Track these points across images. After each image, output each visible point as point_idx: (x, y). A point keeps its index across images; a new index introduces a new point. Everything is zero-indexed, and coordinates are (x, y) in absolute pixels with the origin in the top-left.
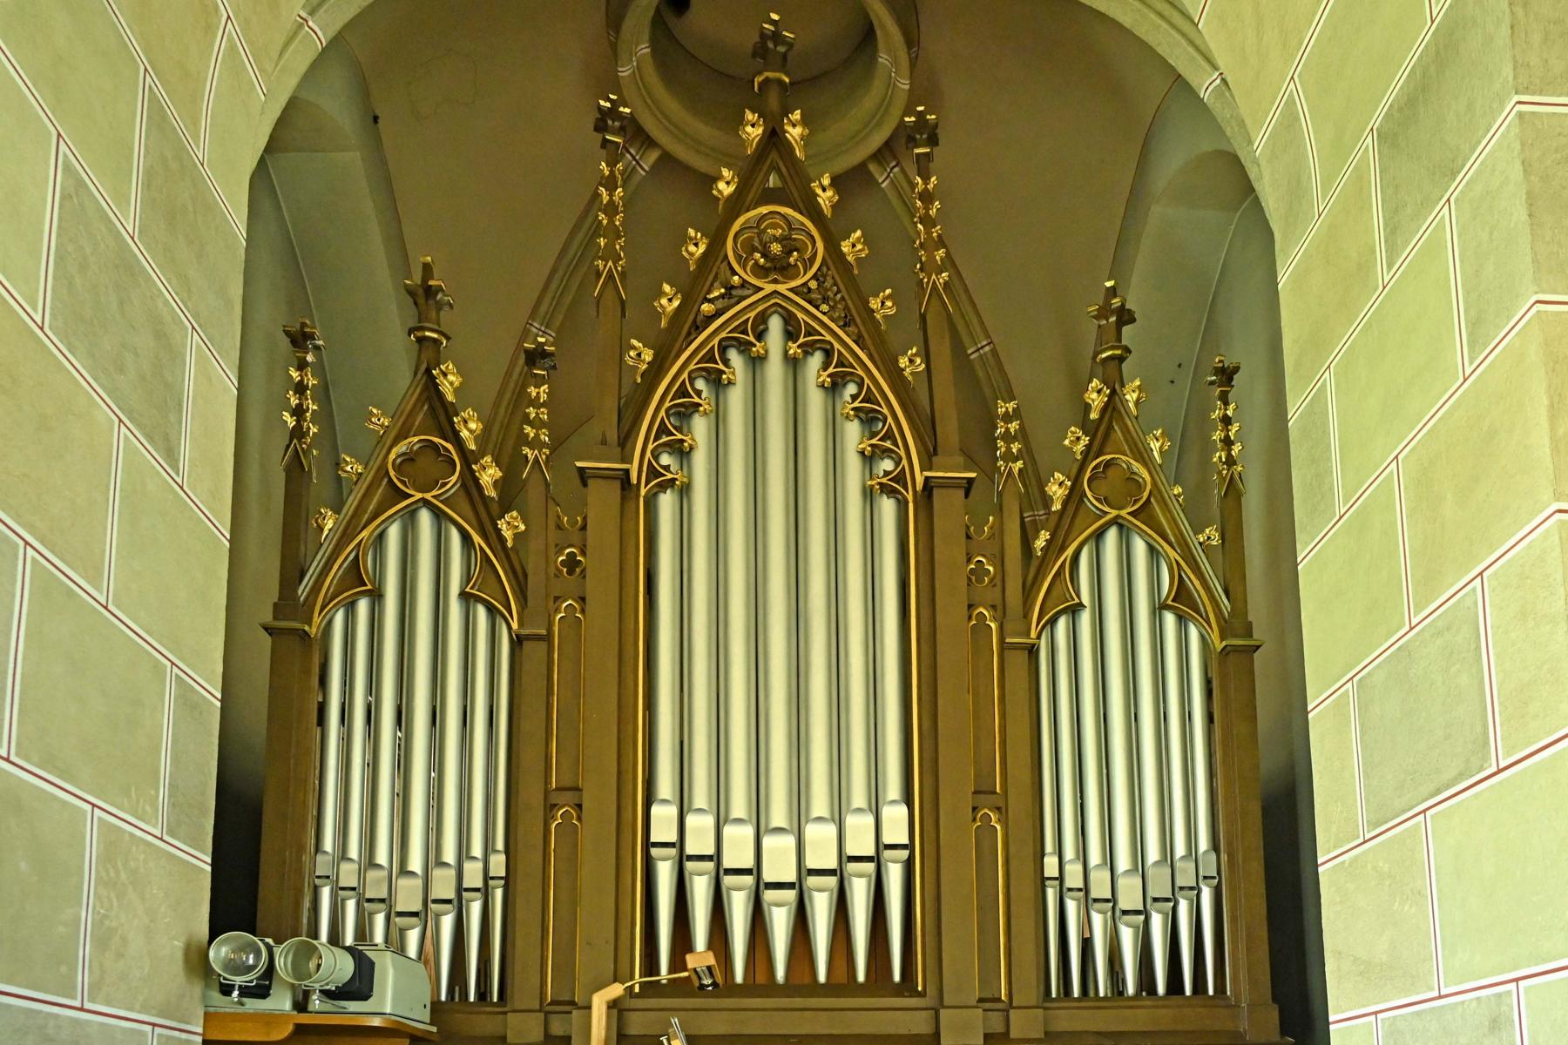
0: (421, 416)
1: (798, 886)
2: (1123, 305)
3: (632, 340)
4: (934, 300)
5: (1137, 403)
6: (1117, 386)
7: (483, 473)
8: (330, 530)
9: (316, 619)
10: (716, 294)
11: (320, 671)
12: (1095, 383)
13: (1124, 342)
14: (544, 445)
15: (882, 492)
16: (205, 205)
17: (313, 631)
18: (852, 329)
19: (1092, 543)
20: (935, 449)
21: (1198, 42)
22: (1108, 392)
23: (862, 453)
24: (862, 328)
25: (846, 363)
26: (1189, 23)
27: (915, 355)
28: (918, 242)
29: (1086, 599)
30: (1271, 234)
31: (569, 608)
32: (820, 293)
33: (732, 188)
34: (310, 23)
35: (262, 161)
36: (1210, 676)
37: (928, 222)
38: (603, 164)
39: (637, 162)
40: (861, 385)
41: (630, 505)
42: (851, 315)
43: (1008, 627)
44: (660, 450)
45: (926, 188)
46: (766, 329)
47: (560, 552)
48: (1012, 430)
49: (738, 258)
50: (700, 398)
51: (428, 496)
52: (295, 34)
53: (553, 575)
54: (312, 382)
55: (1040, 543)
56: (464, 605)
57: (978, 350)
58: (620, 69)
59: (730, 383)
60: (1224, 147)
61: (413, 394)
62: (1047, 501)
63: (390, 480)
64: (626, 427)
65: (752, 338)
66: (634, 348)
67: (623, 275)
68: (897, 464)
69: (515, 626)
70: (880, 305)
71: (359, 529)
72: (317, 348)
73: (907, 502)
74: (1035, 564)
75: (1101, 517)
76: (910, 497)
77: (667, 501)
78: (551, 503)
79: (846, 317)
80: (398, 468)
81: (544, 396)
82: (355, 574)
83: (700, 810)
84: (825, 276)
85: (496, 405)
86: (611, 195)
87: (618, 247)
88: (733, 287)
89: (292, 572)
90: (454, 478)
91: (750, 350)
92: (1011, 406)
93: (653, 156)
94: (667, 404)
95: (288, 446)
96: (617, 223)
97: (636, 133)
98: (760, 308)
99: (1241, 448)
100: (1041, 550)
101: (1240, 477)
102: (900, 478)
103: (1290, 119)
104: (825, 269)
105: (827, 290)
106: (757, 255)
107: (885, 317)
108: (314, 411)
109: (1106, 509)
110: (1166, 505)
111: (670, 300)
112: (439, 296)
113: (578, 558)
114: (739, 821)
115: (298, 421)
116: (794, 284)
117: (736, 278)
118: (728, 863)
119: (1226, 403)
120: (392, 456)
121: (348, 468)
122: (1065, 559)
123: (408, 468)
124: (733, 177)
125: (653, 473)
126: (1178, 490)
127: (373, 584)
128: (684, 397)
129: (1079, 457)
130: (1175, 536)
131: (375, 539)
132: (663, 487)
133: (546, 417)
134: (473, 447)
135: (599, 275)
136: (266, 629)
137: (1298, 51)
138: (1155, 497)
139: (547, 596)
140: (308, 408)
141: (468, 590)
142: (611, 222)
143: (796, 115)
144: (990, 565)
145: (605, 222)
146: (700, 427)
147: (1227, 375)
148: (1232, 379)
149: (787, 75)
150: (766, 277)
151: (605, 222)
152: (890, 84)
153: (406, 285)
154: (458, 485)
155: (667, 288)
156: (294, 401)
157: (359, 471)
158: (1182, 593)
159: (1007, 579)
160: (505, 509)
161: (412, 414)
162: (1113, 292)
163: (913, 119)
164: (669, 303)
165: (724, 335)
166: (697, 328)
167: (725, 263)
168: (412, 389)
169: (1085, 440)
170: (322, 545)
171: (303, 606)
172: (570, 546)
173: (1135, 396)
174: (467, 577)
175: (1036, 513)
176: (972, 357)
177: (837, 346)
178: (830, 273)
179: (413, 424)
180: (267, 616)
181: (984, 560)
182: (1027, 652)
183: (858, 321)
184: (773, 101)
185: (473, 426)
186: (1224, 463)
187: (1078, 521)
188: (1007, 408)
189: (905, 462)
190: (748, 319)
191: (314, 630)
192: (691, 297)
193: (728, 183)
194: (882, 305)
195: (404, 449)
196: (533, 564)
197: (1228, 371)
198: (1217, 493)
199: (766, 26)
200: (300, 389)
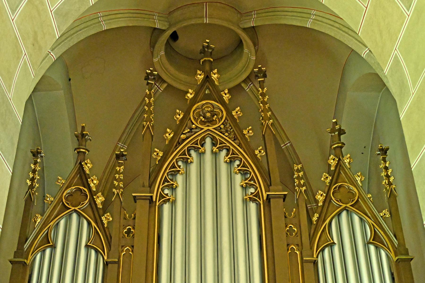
0: (76, 179)
2: (340, 128)
3: (155, 149)
4: (268, 129)
5: (349, 163)
6: (341, 157)
7: (97, 199)
8: (39, 222)
9: (30, 257)
10: (186, 131)
11: (29, 278)
12: (332, 156)
13: (342, 141)
14: (121, 188)
15: (250, 200)
16: (10, 111)
17: (28, 262)
18: (237, 141)
19: (336, 218)
20: (270, 184)
21: (359, 39)
22: (337, 159)
23: (242, 186)
24: (240, 140)
25: (235, 153)
26: (355, 34)
27: (261, 149)
28: (261, 110)
29: (336, 241)
30: (395, 101)
31: (128, 250)
32: (225, 129)
33: (192, 96)
34: (52, 53)
35: (31, 96)
36: (392, 271)
37: (264, 103)
38: (147, 90)
39: (159, 88)
40: (241, 161)
41: (153, 209)
42: (237, 136)
43: (304, 254)
44: (165, 188)
45: (263, 92)
46: (205, 143)
47: (125, 228)
48: (300, 175)
49: (195, 119)
50: (180, 168)
52: (46, 57)
53: (122, 237)
54: (38, 168)
55: (315, 219)
56: (87, 249)
57: (285, 145)
58: (154, 59)
59: (191, 162)
60: (372, 71)
61: (74, 172)
62: (317, 202)
63: (63, 203)
64: (152, 180)
65: (199, 146)
66: (156, 152)
67: (153, 127)
68: (256, 189)
69: (106, 258)
70: (247, 132)
71: (50, 222)
72: (42, 157)
73: (260, 204)
74: (313, 227)
75: (339, 207)
76: (261, 202)
77: (166, 207)
78: (122, 209)
79: (235, 137)
80: (66, 199)
81: (122, 170)
82: (46, 240)
84: (226, 123)
85: (104, 172)
86: (149, 100)
87: (151, 117)
88: (193, 129)
89: (23, 239)
90: (87, 201)
91: (199, 150)
92: (300, 166)
93: (165, 85)
94: (168, 171)
95: (27, 192)
96: (151, 109)
97: (159, 79)
98: (203, 135)
99: (393, 178)
100: (316, 221)
101: (395, 190)
102: (257, 195)
103: (397, 61)
104: (226, 121)
105: (227, 128)
106: (202, 117)
107: (249, 136)
108: (38, 179)
109: (341, 204)
110: (365, 201)
111: (170, 134)
112: (86, 137)
113: (132, 230)
115: (32, 183)
116: (215, 127)
117: (194, 126)
119: (385, 162)
120: (65, 194)
121: (48, 199)
122: (326, 224)
123: (70, 198)
124: (193, 92)
125: (162, 196)
126: (369, 196)
127: (53, 243)
128: (174, 168)
129: (328, 184)
130: (370, 213)
131: (55, 226)
132: (165, 202)
133: (122, 177)
134: (94, 189)
135: (144, 127)
136: (10, 262)
137: (397, 41)
138: (361, 199)
139: (119, 245)
140: (36, 178)
141: (88, 244)
142: (149, 109)
143: (216, 71)
144: (294, 228)
145: (147, 109)
146: (180, 179)
147: (384, 151)
148: (386, 153)
149: (212, 58)
150: (205, 124)
151: (147, 109)
152: (249, 59)
153: (75, 134)
154: (88, 204)
155: (168, 130)
156: (31, 176)
157: (52, 200)
158: (376, 237)
159: (302, 233)
160: (105, 213)
161: (74, 178)
162: (336, 123)
163: (257, 70)
164: (169, 136)
165: (189, 145)
166: (179, 143)
167: (190, 120)
168: (74, 169)
169: (330, 178)
170: (35, 228)
171: (25, 252)
172: (129, 226)
173: (348, 160)
174: (89, 239)
175: (312, 205)
176: (283, 148)
177: (231, 147)
178: (228, 122)
179: (73, 183)
180: (11, 257)
181: (292, 226)
182: (313, 264)
183: (239, 138)
184: (207, 67)
185: (95, 182)
186: (387, 185)
187: (330, 209)
188: (298, 167)
189: (259, 189)
190: (198, 139)
191: (28, 261)
192: (177, 132)
193: (191, 94)
194: (248, 132)
195: (69, 191)
196: (114, 234)
197: (385, 150)
198: (386, 197)
199: (204, 44)
200: (34, 171)
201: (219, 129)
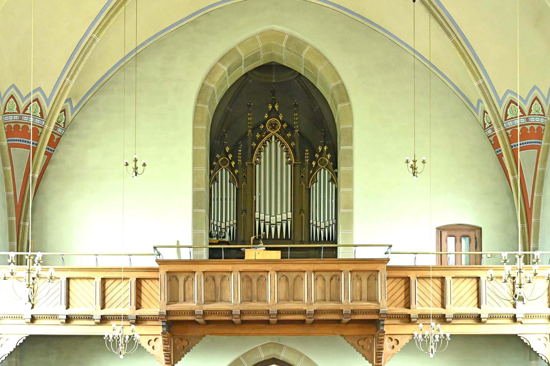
1: (276, 224)
23: (286, 157)
40: (286, 146)
51: (225, 167)
77: (257, 166)
83: (262, 213)
90: (228, 164)
114: (267, 215)
118: (266, 221)
125: (256, 162)
132: (257, 164)
201: (277, 132)
